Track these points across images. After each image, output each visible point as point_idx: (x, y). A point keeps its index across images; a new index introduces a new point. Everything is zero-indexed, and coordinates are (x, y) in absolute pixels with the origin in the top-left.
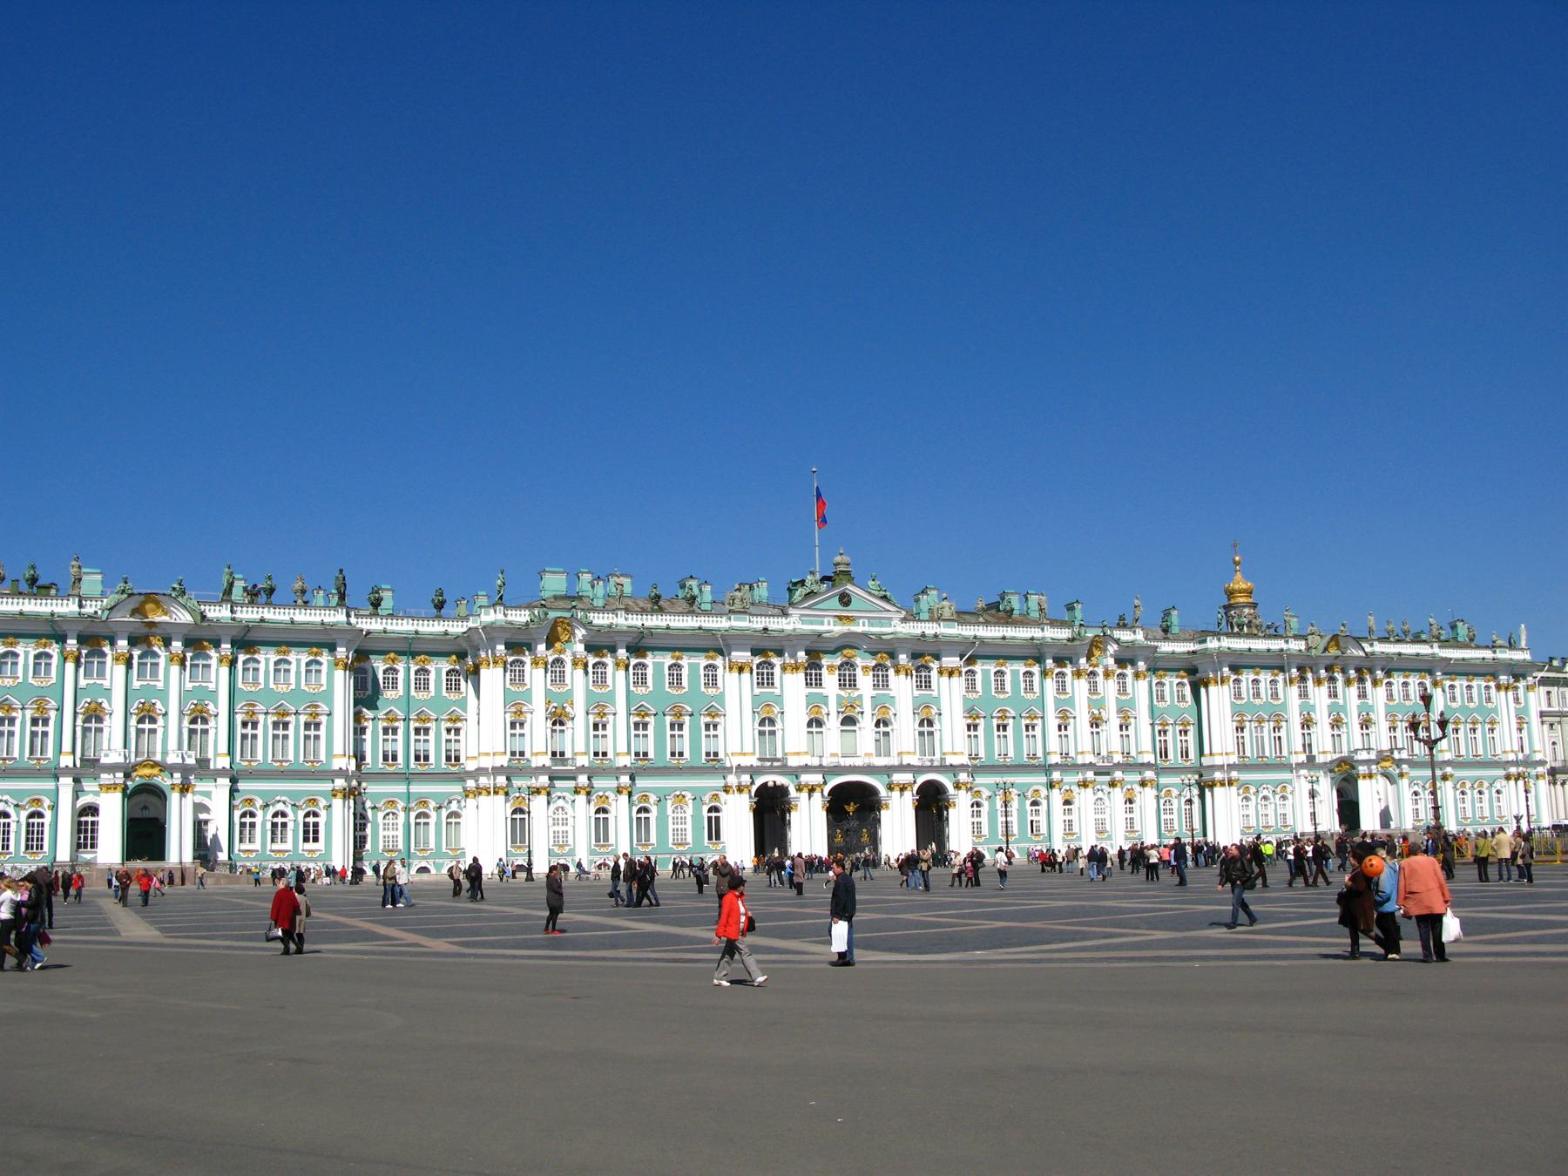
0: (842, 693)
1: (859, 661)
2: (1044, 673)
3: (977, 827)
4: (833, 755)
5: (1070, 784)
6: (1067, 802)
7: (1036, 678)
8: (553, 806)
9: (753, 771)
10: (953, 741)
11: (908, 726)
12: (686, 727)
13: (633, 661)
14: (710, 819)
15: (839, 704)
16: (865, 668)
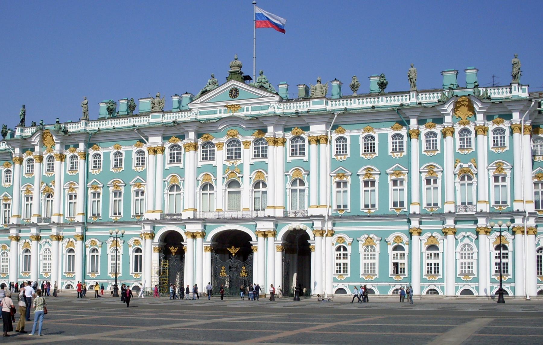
0: (228, 164)
1: (241, 139)
2: (409, 136)
3: (341, 269)
4: (218, 210)
5: (432, 231)
6: (432, 247)
7: (405, 139)
8: (43, 248)
9: (153, 223)
10: (322, 195)
11: (281, 184)
12: (122, 194)
13: (92, 152)
14: (136, 257)
15: (224, 173)
16: (247, 144)
